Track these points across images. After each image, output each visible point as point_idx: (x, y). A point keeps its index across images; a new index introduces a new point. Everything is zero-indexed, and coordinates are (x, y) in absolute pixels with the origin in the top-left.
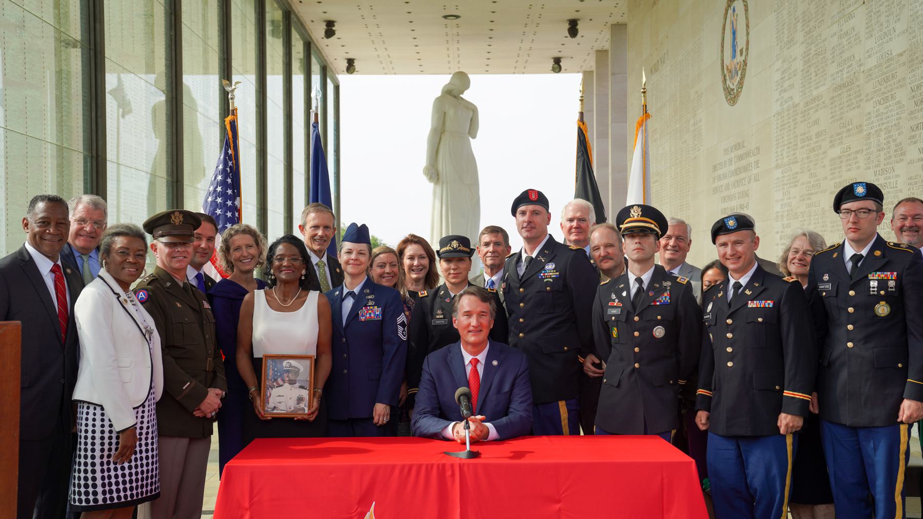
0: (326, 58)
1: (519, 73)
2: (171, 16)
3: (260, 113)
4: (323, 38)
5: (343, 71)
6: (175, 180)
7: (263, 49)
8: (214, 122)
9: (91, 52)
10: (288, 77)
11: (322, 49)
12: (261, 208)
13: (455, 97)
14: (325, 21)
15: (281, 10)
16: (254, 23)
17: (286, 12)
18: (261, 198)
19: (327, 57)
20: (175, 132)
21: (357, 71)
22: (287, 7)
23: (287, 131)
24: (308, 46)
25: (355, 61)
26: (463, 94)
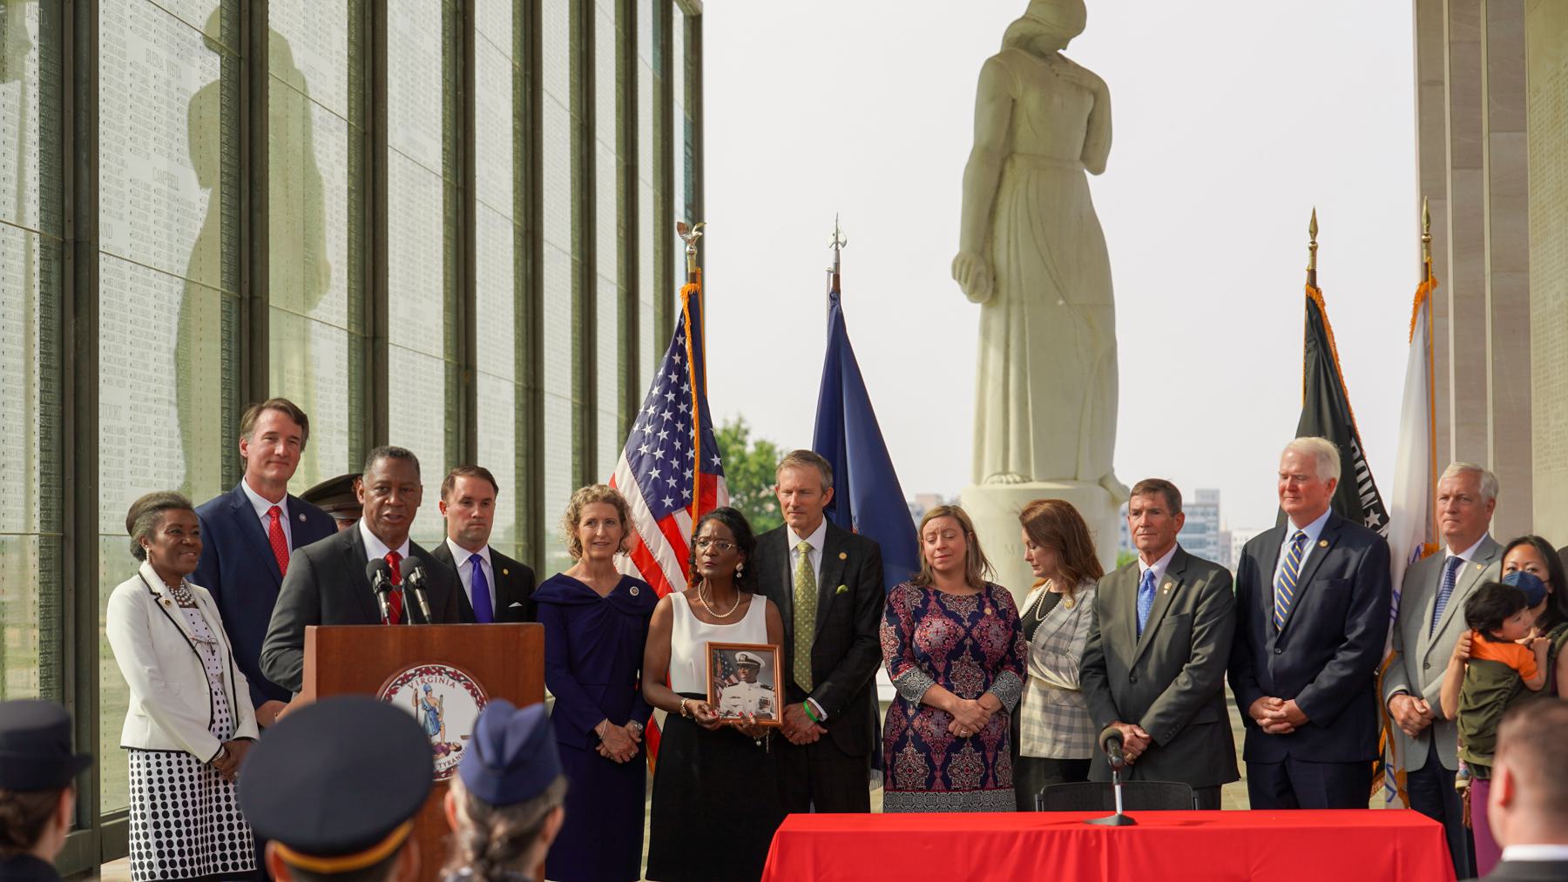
3: (525, 135)
9: (242, 64)
10: (584, 22)
12: (527, 389)
13: (1042, 55)
18: (527, 361)
20: (371, 216)
23: (582, 170)
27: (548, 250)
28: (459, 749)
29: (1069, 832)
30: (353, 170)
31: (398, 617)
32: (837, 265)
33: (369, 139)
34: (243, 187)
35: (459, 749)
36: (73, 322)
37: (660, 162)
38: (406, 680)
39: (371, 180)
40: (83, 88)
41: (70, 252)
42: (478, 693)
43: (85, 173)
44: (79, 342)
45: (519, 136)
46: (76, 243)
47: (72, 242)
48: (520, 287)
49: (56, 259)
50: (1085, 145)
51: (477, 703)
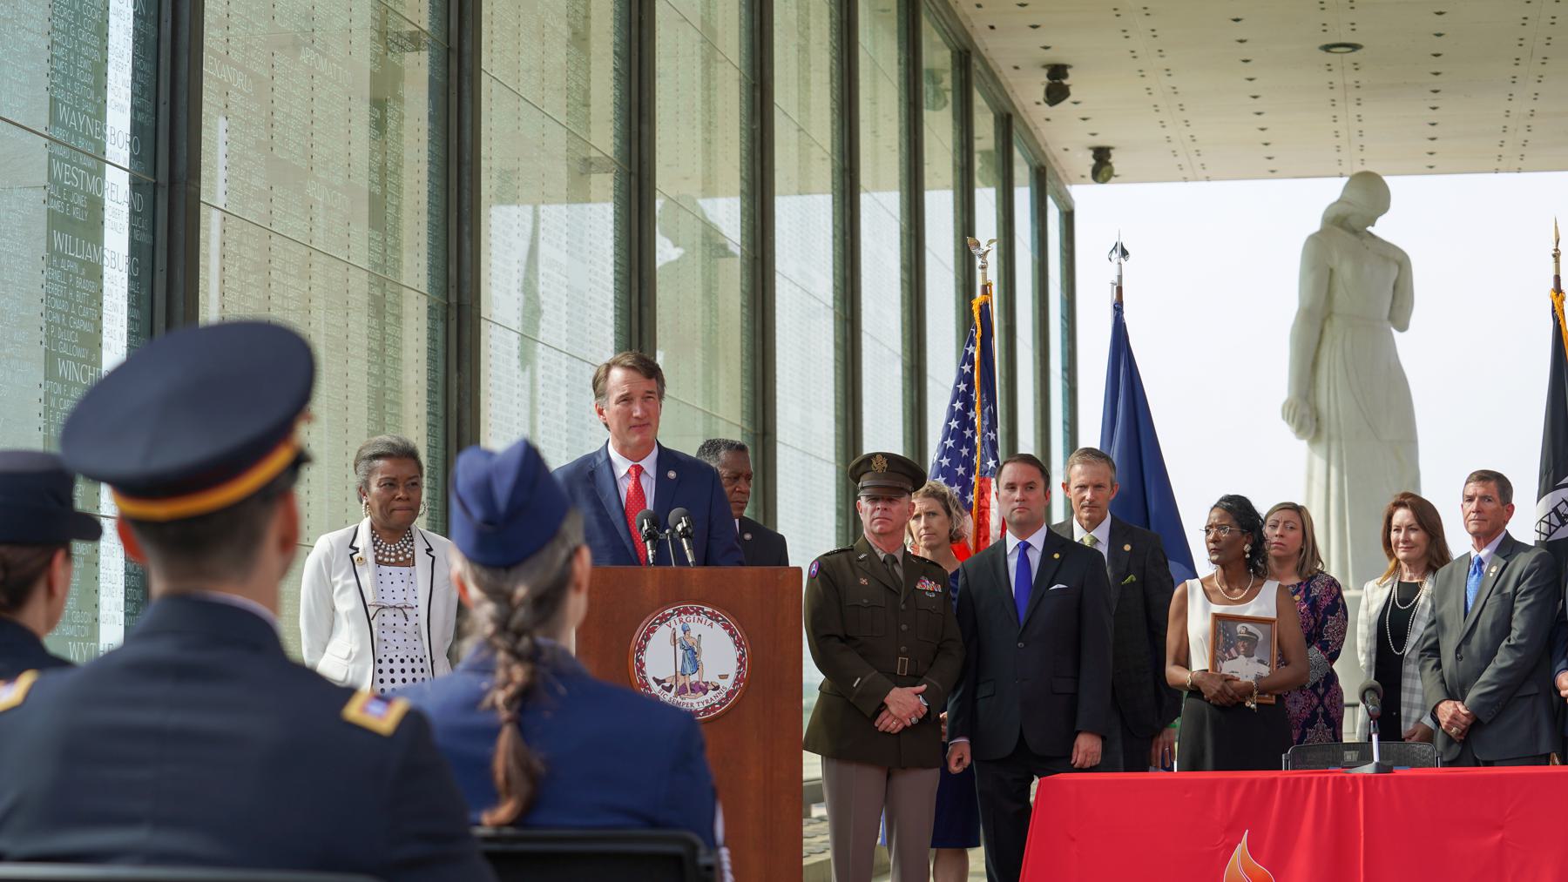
0: (1043, 148)
1: (1508, 171)
2: (754, 91)
3: (910, 283)
4: (1038, 103)
5: (1083, 176)
6: (759, 431)
7: (916, 141)
8: (827, 306)
11: (1036, 128)
13: (1355, 232)
14: (1045, 66)
15: (950, 48)
16: (896, 83)
17: (960, 53)
19: (1046, 145)
21: (1116, 176)
22: (964, 41)
24: (1006, 123)
25: (1112, 152)
26: (1372, 223)
27: (930, 384)
28: (717, 688)
29: (1327, 778)
30: (744, 288)
31: (661, 559)
32: (1120, 277)
33: (759, 263)
34: (633, 285)
35: (717, 688)
36: (456, 376)
37: (1037, 328)
38: (664, 619)
39: (761, 299)
40: (466, 169)
41: (453, 314)
42: (736, 634)
43: (467, 245)
44: (462, 394)
45: (906, 285)
46: (459, 306)
47: (455, 306)
48: (907, 413)
49: (442, 320)
50: (1391, 308)
51: (735, 643)
